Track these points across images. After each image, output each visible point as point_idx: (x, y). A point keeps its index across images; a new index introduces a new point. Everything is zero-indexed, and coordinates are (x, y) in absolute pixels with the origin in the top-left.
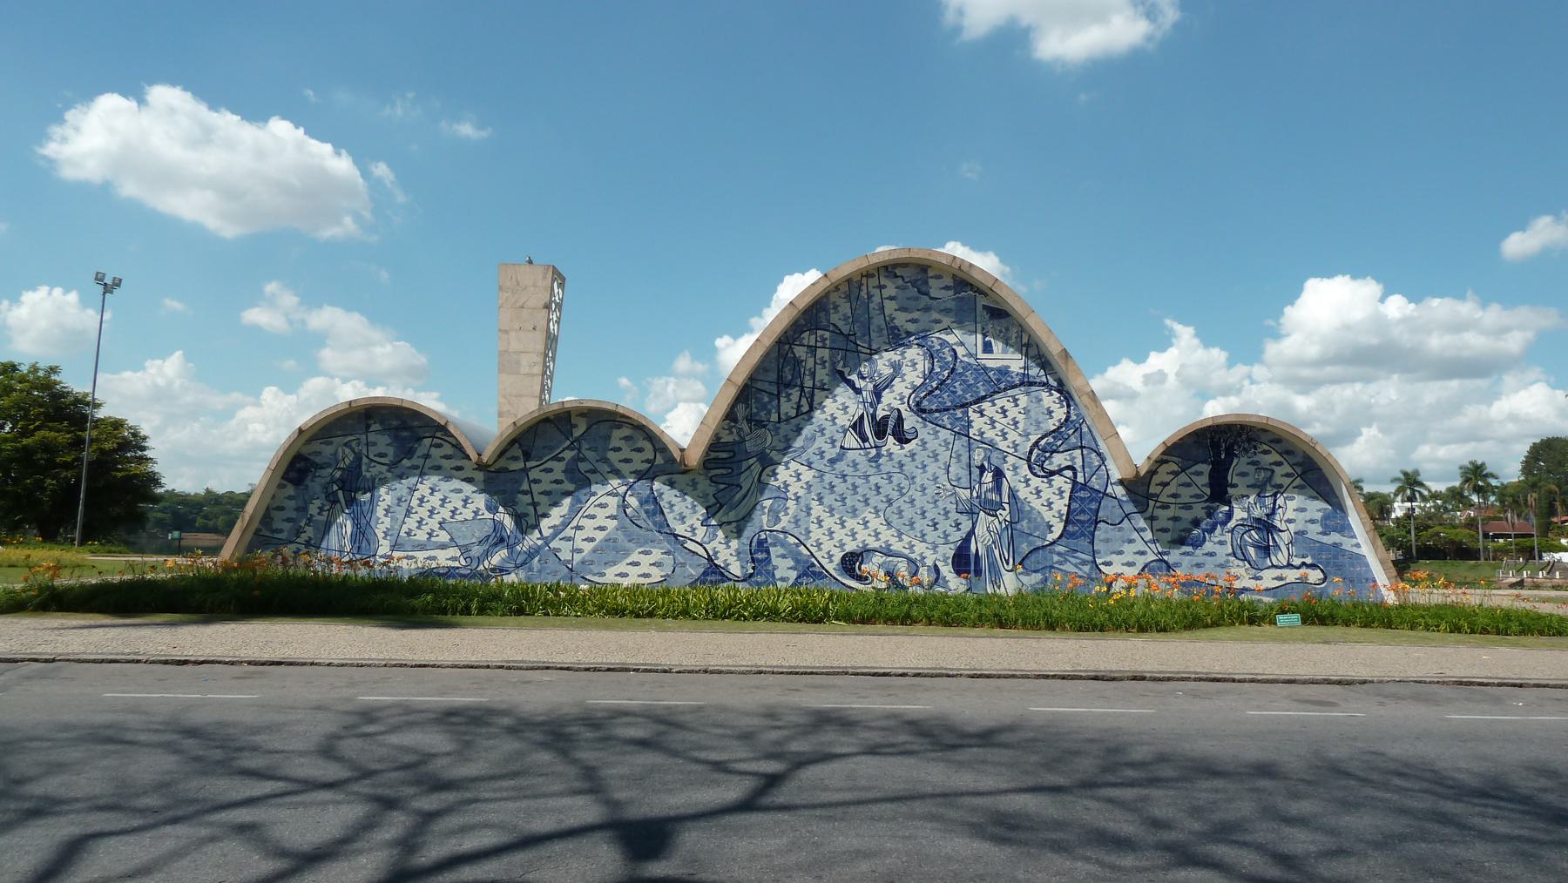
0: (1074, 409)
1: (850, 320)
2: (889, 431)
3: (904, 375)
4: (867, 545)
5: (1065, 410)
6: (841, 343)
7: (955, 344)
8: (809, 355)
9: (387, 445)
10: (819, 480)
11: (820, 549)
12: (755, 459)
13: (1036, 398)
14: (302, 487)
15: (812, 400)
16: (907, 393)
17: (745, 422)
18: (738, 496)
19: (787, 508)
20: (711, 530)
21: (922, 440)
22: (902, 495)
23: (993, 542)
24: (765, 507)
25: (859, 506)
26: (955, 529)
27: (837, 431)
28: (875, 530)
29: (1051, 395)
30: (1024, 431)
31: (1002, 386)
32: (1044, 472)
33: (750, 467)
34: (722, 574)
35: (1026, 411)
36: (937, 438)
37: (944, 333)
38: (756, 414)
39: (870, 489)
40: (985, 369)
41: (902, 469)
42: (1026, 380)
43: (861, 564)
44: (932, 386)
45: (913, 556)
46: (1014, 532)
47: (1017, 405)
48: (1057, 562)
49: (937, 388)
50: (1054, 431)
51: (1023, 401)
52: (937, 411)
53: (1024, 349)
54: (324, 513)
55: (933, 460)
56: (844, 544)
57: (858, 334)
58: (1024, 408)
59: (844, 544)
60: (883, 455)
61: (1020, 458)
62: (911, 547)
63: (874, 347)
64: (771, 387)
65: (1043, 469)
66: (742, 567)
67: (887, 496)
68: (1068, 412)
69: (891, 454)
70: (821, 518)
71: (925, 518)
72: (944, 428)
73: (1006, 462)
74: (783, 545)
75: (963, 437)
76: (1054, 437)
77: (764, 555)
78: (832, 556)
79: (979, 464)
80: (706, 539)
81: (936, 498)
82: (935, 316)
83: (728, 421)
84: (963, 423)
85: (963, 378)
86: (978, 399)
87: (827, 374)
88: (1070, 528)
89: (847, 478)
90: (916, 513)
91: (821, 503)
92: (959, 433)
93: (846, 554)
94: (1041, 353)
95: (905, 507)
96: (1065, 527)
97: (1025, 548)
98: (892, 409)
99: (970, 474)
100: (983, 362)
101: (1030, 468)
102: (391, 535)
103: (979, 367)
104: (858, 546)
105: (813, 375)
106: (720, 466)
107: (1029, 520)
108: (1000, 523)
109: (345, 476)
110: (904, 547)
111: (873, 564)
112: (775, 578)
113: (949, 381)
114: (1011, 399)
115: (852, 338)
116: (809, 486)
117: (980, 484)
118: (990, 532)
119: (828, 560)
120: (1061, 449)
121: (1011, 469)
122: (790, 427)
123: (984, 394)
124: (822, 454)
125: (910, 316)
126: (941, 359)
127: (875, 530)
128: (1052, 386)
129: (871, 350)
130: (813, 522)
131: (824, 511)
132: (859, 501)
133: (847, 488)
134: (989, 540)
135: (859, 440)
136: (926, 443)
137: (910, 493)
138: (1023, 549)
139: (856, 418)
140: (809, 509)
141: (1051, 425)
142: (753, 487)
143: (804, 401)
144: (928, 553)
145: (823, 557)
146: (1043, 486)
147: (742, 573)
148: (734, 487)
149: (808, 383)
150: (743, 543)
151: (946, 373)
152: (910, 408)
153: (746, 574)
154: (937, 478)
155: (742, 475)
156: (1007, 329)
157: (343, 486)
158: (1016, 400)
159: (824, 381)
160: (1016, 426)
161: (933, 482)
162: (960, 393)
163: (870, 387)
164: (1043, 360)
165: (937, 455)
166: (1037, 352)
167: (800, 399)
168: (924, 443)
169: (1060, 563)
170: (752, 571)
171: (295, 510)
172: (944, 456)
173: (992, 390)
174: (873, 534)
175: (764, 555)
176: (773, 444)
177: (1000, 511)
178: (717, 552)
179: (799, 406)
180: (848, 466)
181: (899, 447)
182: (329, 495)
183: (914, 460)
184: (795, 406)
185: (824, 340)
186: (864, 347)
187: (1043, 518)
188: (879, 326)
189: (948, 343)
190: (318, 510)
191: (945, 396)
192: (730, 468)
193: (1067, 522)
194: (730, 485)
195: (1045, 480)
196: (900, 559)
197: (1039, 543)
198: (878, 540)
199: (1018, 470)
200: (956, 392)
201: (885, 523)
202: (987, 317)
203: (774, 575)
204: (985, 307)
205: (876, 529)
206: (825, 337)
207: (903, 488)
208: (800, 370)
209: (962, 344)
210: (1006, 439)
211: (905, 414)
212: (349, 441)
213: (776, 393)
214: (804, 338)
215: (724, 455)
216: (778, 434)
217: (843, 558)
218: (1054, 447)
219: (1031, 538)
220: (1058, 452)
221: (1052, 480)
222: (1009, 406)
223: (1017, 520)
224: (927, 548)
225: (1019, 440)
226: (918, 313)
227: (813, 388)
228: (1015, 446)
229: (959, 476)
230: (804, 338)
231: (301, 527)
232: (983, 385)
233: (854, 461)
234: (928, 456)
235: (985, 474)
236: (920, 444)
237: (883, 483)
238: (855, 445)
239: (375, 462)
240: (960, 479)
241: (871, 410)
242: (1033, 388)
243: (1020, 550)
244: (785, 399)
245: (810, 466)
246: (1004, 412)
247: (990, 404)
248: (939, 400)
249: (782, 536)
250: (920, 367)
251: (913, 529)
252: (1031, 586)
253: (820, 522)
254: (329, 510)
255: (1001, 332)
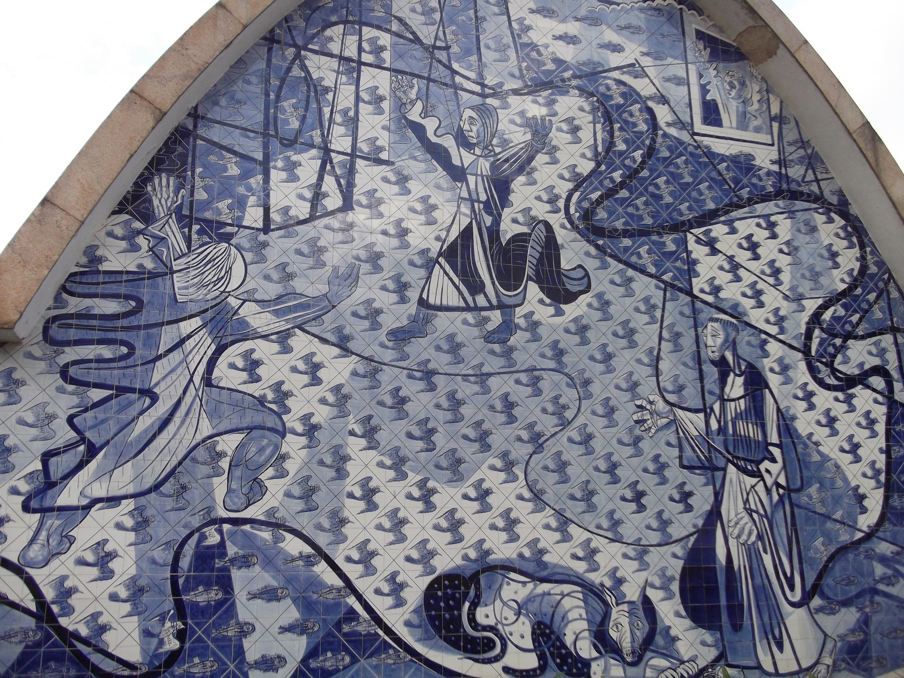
0: (872, 253)
1: (437, 16)
2: (529, 271)
3: (555, 148)
4: (488, 553)
5: (856, 252)
6: (416, 61)
7: (650, 98)
8: (344, 78)
10: (366, 382)
11: (370, 570)
12: (196, 322)
13: (807, 223)
15: (351, 185)
16: (564, 188)
17: (173, 222)
18: (145, 423)
19: (283, 457)
20: (54, 522)
21: (599, 296)
22: (565, 424)
23: (760, 537)
24: (221, 455)
25: (468, 451)
26: (681, 507)
27: (412, 263)
28: (506, 514)
29: (830, 221)
30: (791, 289)
31: (745, 193)
32: (837, 378)
33: (182, 342)
34: (82, 661)
35: (791, 249)
36: (630, 294)
37: (629, 73)
38: (207, 204)
39: (492, 408)
40: (710, 154)
41: (559, 362)
42: (785, 186)
43: (474, 605)
44: (612, 180)
45: (595, 578)
46: (796, 510)
47: (774, 236)
48: (883, 579)
49: (622, 185)
50: (843, 294)
51: (784, 227)
52: (626, 233)
53: (775, 125)
55: (624, 342)
56: (432, 554)
57: (455, 49)
58: (788, 243)
59: (432, 554)
60: (517, 327)
61: (791, 347)
62: (591, 554)
63: (490, 81)
64: (243, 141)
65: (834, 371)
66: (147, 633)
67: (531, 426)
68: (862, 259)
69: (536, 324)
70: (372, 484)
71: (615, 480)
72: (643, 271)
73: (766, 355)
74: (268, 563)
75: (682, 296)
76: (844, 306)
77: (215, 595)
78: (402, 586)
79: (716, 356)
80: (36, 552)
81: (637, 432)
82: (610, 36)
83: (125, 217)
84: (679, 264)
85: (672, 169)
86: (703, 216)
87: (384, 128)
88: (896, 501)
89: (436, 379)
90: (597, 469)
91: (373, 445)
92: (673, 286)
93: (437, 580)
94: (805, 140)
95: (572, 453)
96: (886, 498)
97: (820, 549)
98: (534, 222)
99: (701, 378)
100: (706, 141)
101: (812, 370)
103: (699, 151)
104: (466, 557)
105: (353, 123)
106: (96, 335)
107: (822, 485)
108: (768, 490)
110: (575, 557)
111: (505, 604)
112: (243, 660)
113: (645, 173)
114: (764, 225)
115: (442, 55)
116: (341, 398)
117: (723, 400)
118: (750, 512)
119: (390, 601)
120: (860, 331)
121: (777, 369)
122: (289, 244)
123: (711, 206)
124: (373, 315)
125: (561, 28)
126: (627, 125)
127: (506, 514)
128: (830, 204)
129: (483, 86)
130: (351, 496)
131: (381, 465)
132: (465, 437)
133: (438, 406)
134: (750, 534)
135: (462, 287)
136: (607, 303)
137: (580, 420)
138: (817, 550)
139: (454, 233)
140: (341, 459)
141: (838, 281)
142: (188, 399)
143: (329, 184)
144: (628, 568)
145: (378, 592)
146: (838, 409)
147: (144, 651)
148: (136, 396)
149: (340, 142)
150: (154, 562)
151: (638, 155)
152: (571, 222)
153: (155, 656)
154: (636, 385)
155: (164, 361)
156: (743, 84)
158: (771, 226)
159: (378, 143)
160: (777, 279)
161: (628, 395)
162: (668, 199)
163: (485, 166)
164: (809, 151)
165: (632, 332)
166: (798, 137)
167: (321, 178)
168: (604, 305)
169: (888, 580)
170: (174, 644)
172: (647, 336)
173: (726, 201)
174: (501, 523)
175: (215, 595)
176: (250, 285)
177: (766, 465)
178: (70, 592)
179: (318, 196)
180: (438, 348)
181: (551, 310)
183: (584, 342)
184: (308, 195)
185: (378, 50)
186: (468, 78)
187: (845, 480)
188: (498, 39)
189: (638, 94)
191: (639, 202)
192: (123, 343)
193: (889, 488)
194: (122, 390)
195: (841, 396)
196: (567, 588)
197: (845, 537)
198: (514, 538)
199: (791, 373)
200: (659, 198)
201: (527, 494)
202: (706, 54)
203: (240, 652)
204: (700, 35)
205: (509, 511)
206: (381, 42)
207: (564, 407)
208: (320, 110)
209: (663, 100)
210: (761, 305)
211: (562, 235)
213: (259, 156)
214: (331, 39)
215: (110, 307)
216: (262, 259)
217: (430, 593)
218: (848, 327)
219: (829, 525)
220: (856, 338)
221: (852, 396)
222: (760, 235)
223: (799, 483)
224: (625, 556)
225: (786, 308)
226: (578, 24)
227: (353, 154)
228: (781, 321)
229: (681, 380)
230: (331, 39)
232: (710, 188)
233: (451, 337)
234: (615, 334)
235: (730, 379)
236: (596, 304)
237: (520, 393)
238: (453, 299)
240: (680, 389)
241: (488, 220)
242: (800, 205)
243: (811, 553)
244: (284, 175)
245: (343, 344)
246: (753, 247)
247: (726, 229)
248: (630, 210)
249: (266, 535)
250: (586, 135)
251: (591, 508)
252: (842, 637)
253: (369, 495)
255: (732, 87)
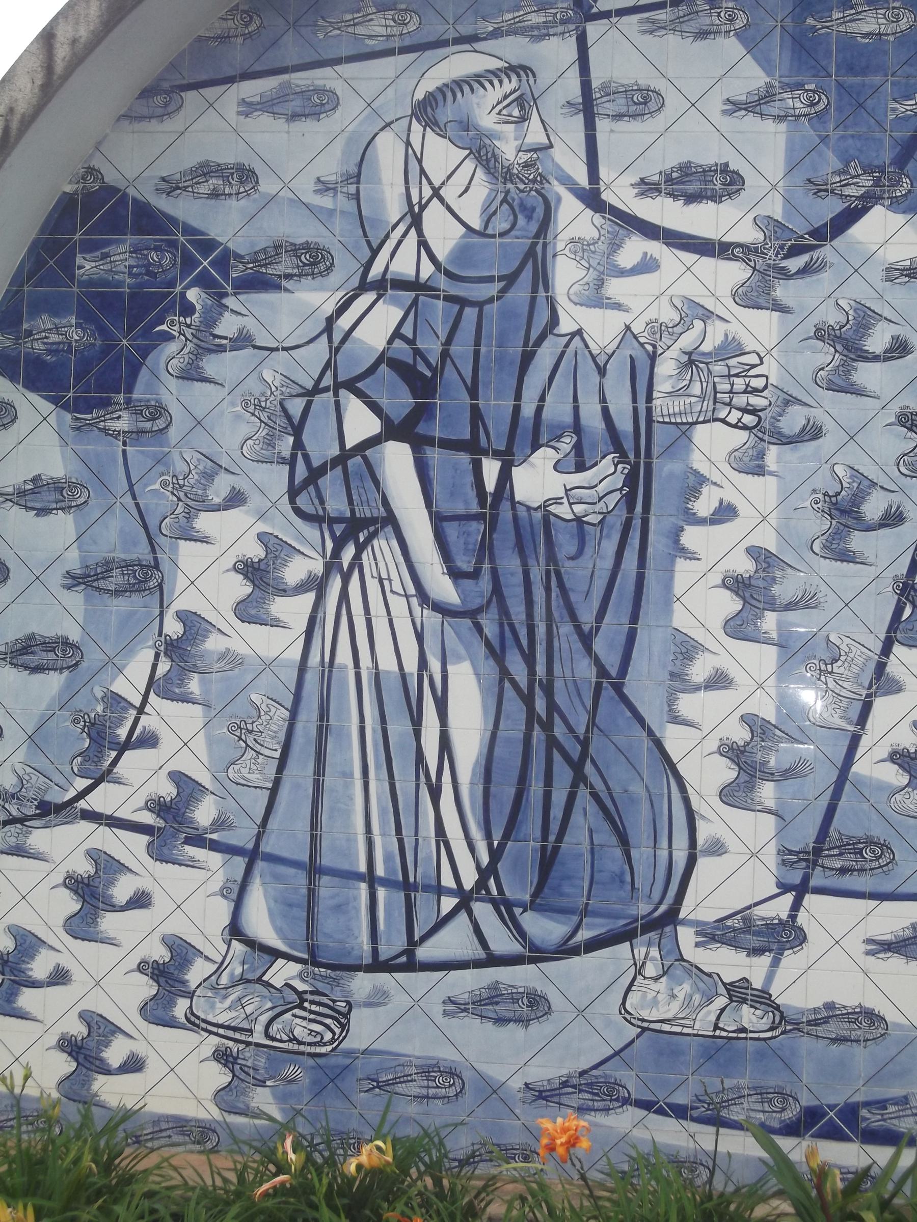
9: (734, 107)
14: (124, 423)
54: (280, 606)
102: (788, 774)
109: (432, 347)
157: (421, 412)
171: (74, 580)
182: (316, 474)
190: (241, 588)
212: (458, 85)
231: (116, 701)
239: (650, 231)
254: (318, 585)
